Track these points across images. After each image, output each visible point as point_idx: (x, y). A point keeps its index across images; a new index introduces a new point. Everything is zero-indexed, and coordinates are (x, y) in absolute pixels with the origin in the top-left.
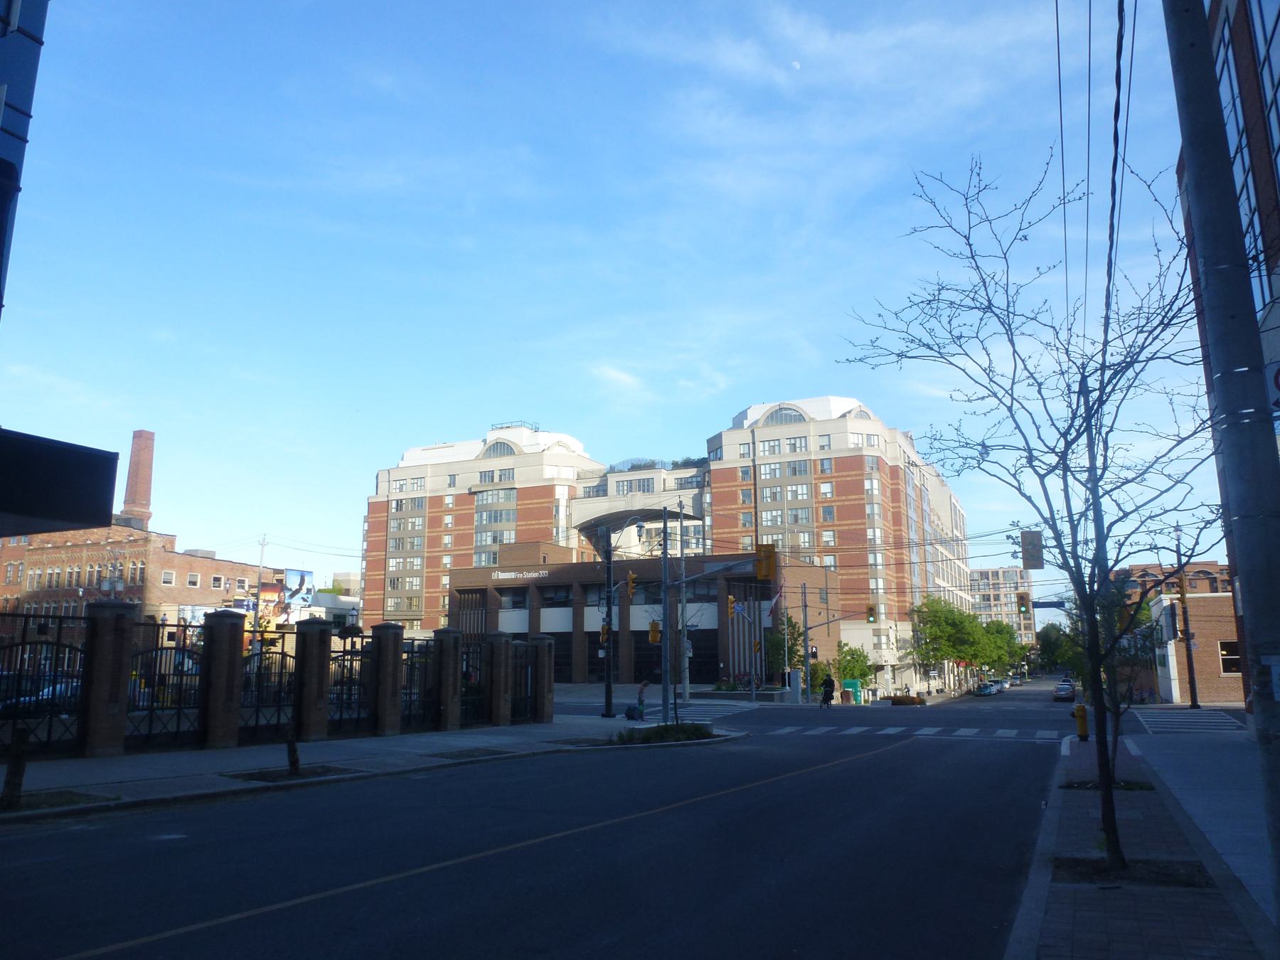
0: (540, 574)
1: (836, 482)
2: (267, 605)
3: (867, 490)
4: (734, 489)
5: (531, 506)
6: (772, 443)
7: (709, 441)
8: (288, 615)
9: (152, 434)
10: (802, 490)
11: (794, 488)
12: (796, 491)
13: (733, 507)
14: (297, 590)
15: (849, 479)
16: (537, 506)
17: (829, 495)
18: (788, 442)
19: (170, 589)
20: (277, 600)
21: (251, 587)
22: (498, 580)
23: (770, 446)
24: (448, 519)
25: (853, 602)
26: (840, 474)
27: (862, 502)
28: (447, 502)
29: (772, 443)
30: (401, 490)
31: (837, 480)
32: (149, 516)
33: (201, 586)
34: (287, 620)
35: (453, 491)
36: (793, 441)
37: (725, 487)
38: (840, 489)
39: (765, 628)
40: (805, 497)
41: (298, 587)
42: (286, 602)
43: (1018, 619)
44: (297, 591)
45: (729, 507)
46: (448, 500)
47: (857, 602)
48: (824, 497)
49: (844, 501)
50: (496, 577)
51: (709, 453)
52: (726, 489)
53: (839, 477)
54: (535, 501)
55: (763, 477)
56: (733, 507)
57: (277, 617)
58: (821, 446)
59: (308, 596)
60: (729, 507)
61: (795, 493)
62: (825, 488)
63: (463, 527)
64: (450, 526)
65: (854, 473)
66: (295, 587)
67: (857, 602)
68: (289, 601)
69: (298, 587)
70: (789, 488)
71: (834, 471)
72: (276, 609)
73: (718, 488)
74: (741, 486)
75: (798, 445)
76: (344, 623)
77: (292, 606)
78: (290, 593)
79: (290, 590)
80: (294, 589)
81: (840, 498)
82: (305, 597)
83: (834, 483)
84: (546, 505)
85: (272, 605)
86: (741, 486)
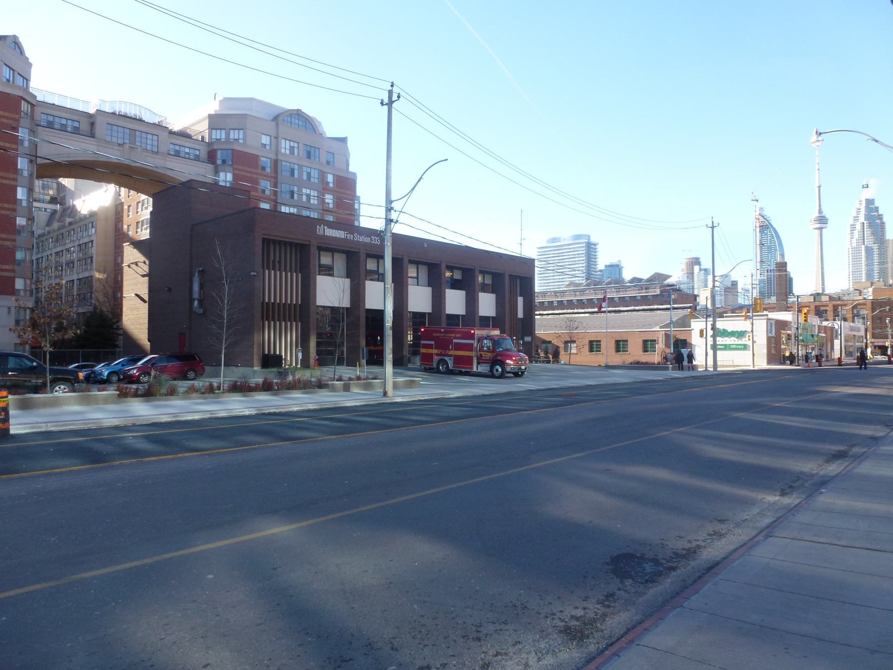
0: (371, 239)
1: (337, 196)
3: (356, 209)
4: (255, 176)
6: (292, 144)
11: (308, 191)
17: (331, 206)
22: (324, 237)
23: (290, 146)
27: (353, 218)
31: (338, 194)
36: (309, 149)
37: (247, 172)
38: (339, 203)
48: (327, 206)
50: (321, 233)
52: (248, 174)
53: (339, 192)
55: (284, 173)
58: (327, 161)
62: (329, 199)
70: (304, 190)
71: (335, 186)
73: (240, 170)
74: (262, 175)
75: (312, 154)
83: (335, 197)
86: (262, 175)
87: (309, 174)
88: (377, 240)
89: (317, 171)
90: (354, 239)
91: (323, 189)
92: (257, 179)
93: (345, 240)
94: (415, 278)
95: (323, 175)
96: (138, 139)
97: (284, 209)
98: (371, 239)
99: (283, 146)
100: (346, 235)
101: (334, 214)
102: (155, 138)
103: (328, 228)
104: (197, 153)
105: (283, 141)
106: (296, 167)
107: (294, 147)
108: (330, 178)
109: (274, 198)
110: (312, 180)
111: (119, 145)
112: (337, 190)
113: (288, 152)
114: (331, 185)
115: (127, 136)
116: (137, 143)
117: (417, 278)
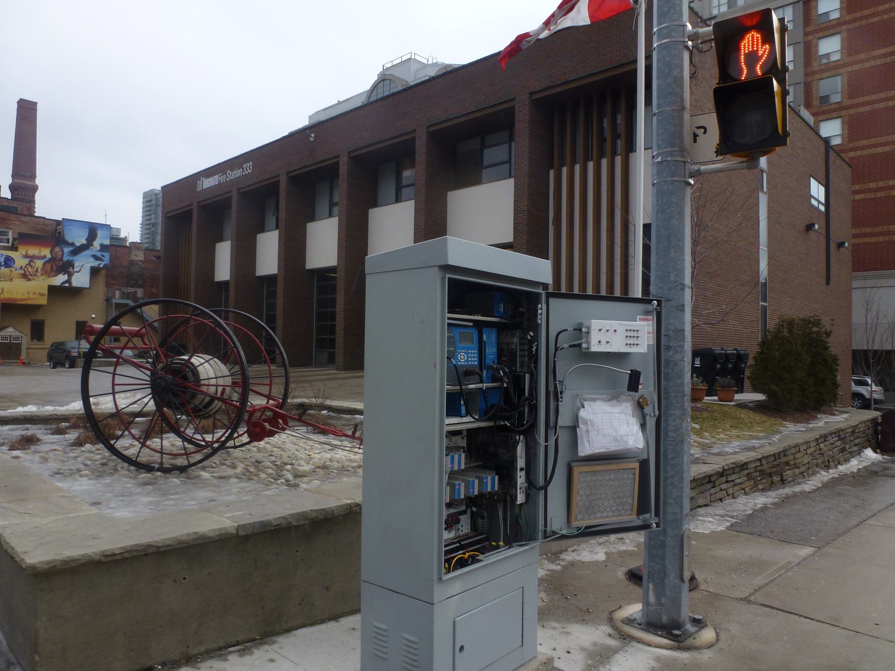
2: (30, 261)
8: (70, 275)
9: (35, 104)
20: (49, 256)
25: (873, 240)
26: (858, 14)
32: (35, 189)
34: (69, 281)
41: (84, 241)
42: (66, 258)
47: (881, 239)
48: (824, 61)
49: (863, 61)
57: (49, 277)
59: (103, 254)
66: (81, 240)
67: (881, 239)
69: (84, 241)
77: (76, 264)
78: (70, 249)
79: (72, 244)
80: (78, 244)
81: (855, 58)
83: (845, 34)
85: (39, 264)
88: (250, 169)
90: (226, 179)
91: (806, 34)
93: (220, 184)
98: (243, 171)
100: (220, 178)
101: (841, 71)
103: (206, 179)
112: (848, 18)
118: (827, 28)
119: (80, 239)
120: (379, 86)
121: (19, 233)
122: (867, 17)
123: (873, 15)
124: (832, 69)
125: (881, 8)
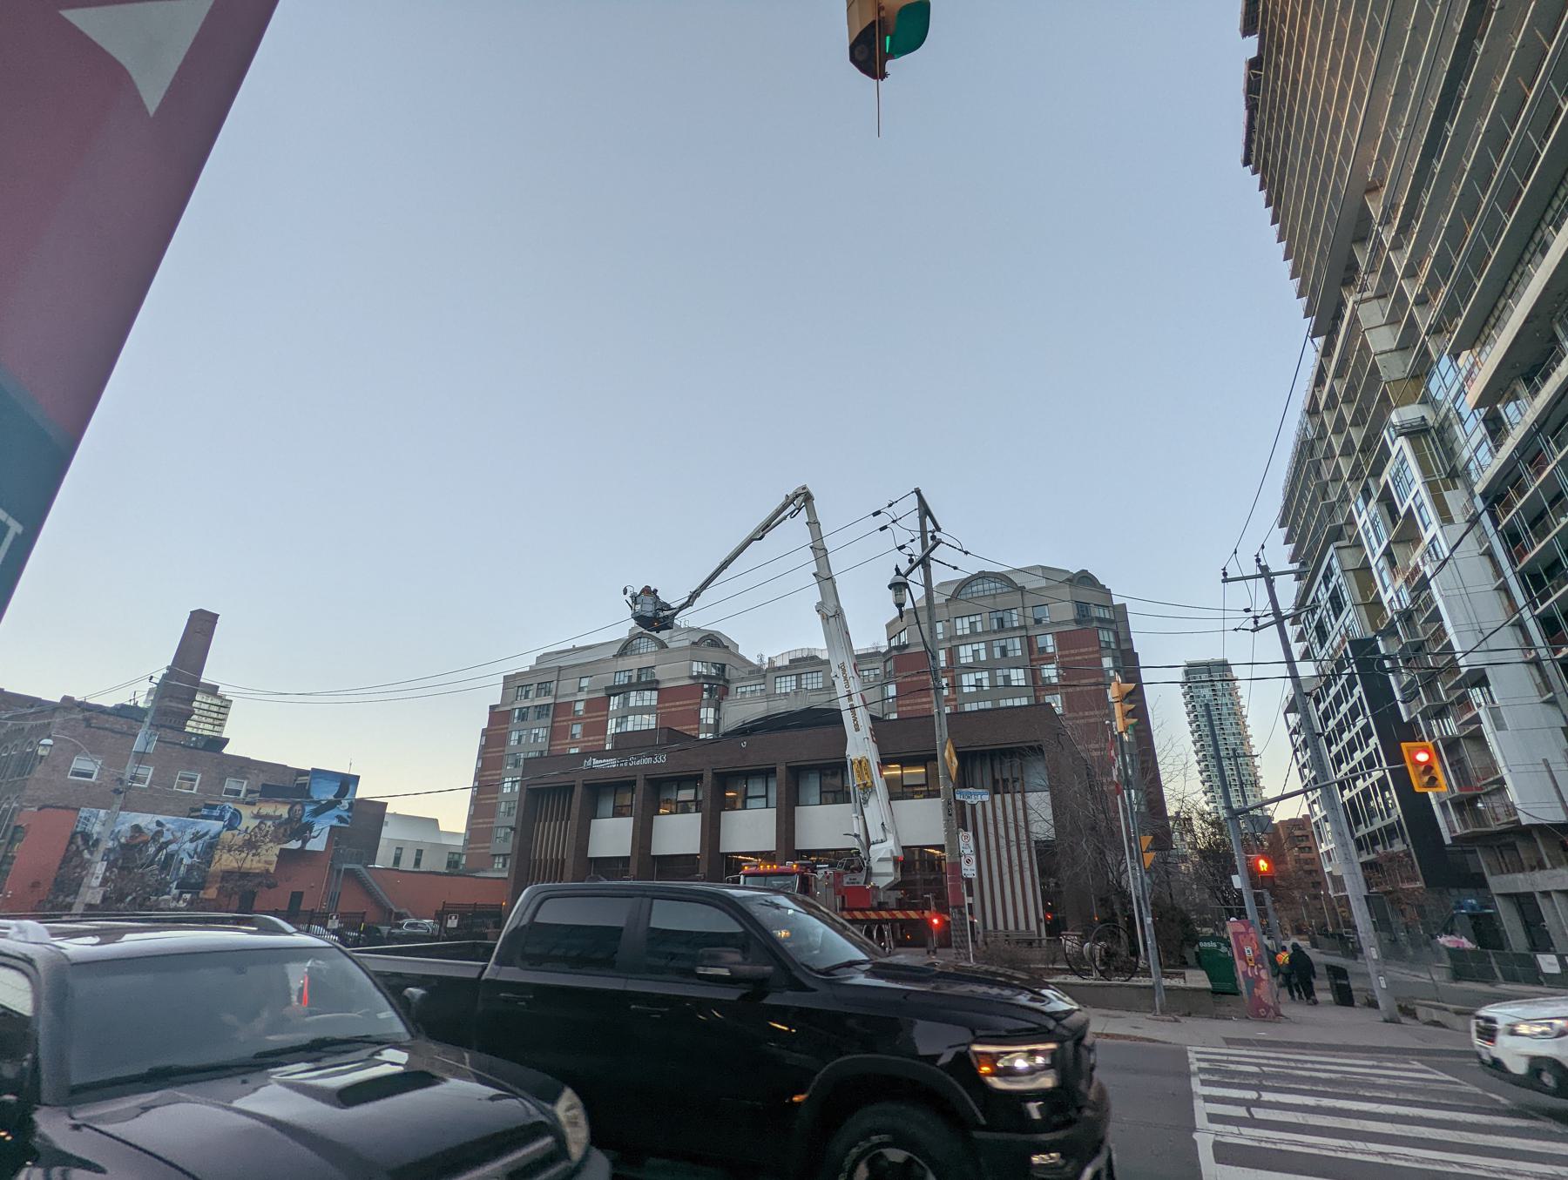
5: (673, 709)
6: (972, 619)
7: (888, 626)
10: (1018, 677)
11: (1006, 672)
12: (1009, 676)
13: (924, 700)
14: (329, 802)
15: (1077, 658)
16: (680, 709)
18: (993, 615)
19: (87, 786)
21: (249, 792)
23: (970, 623)
24: (577, 729)
26: (1067, 652)
28: (577, 709)
29: (972, 619)
30: (526, 697)
33: (151, 782)
35: (583, 696)
36: (1000, 615)
39: (1036, 842)
40: (1023, 683)
41: (331, 797)
43: (1405, 848)
44: (331, 805)
45: (919, 701)
46: (580, 706)
48: (1047, 682)
51: (889, 640)
54: (678, 703)
55: (963, 661)
56: (924, 700)
60: (919, 701)
61: (1007, 678)
62: (1050, 672)
63: (591, 738)
64: (578, 736)
65: (1086, 650)
68: (311, 820)
70: (999, 672)
72: (282, 830)
76: (258, 826)
82: (345, 815)
84: (691, 707)
87: (1004, 650)
89: (1017, 641)
91: (1031, 660)
92: (928, 680)
94: (762, 797)
95: (1029, 642)
96: (804, 682)
97: (968, 708)
99: (959, 625)
102: (820, 674)
104: (878, 672)
105: (958, 621)
106: (982, 646)
107: (975, 622)
108: (1049, 643)
109: (954, 696)
110: (1010, 654)
111: (786, 694)
113: (967, 632)
114: (1050, 650)
115: (794, 683)
116: (804, 686)
117: (766, 796)
118: (1046, 659)
119: (326, 793)
120: (634, 642)
121: (264, 785)
122: (1074, 655)
123: (1077, 655)
124: (1052, 689)
125: (1082, 650)
